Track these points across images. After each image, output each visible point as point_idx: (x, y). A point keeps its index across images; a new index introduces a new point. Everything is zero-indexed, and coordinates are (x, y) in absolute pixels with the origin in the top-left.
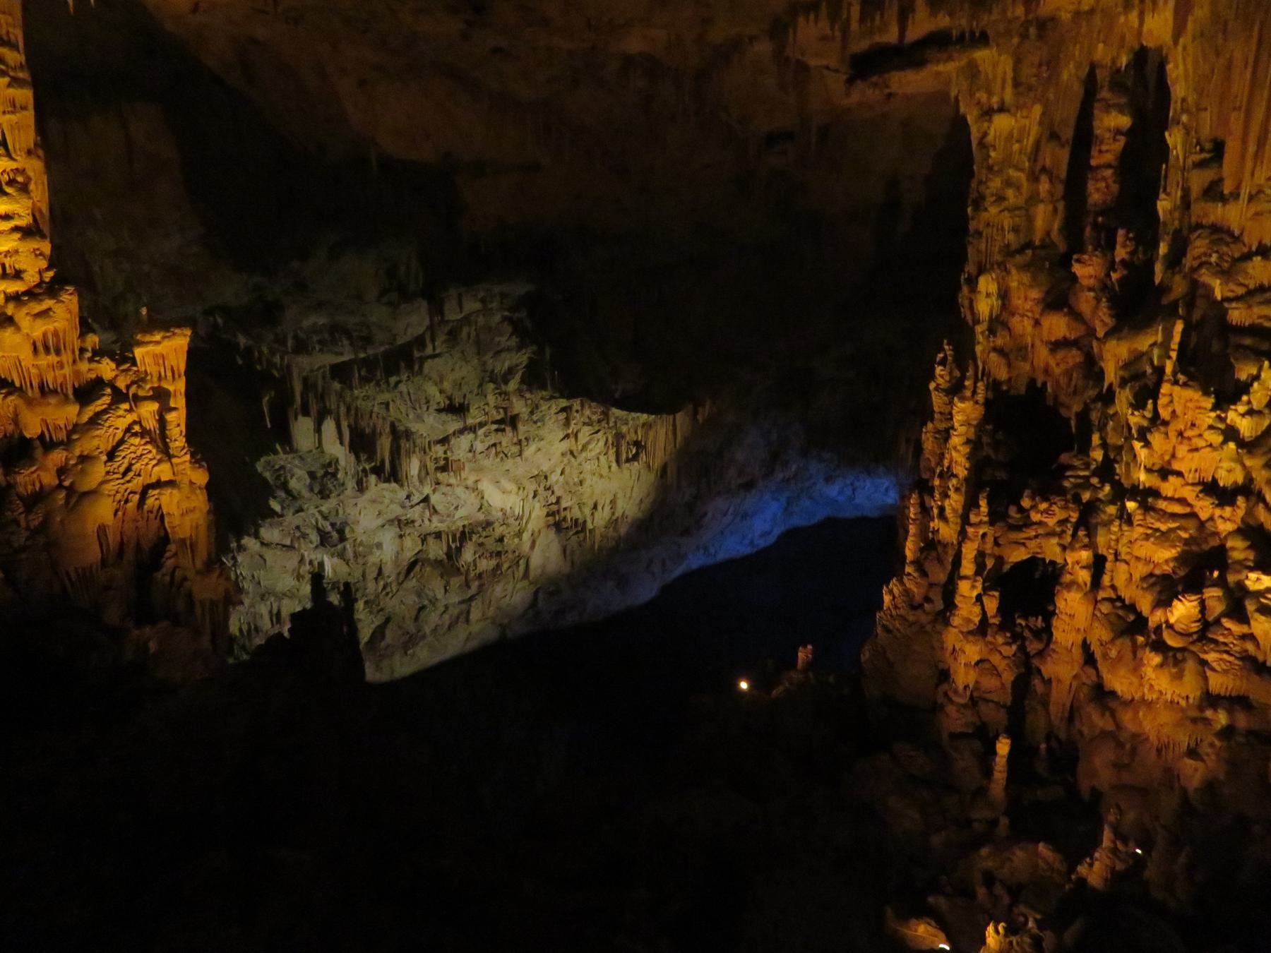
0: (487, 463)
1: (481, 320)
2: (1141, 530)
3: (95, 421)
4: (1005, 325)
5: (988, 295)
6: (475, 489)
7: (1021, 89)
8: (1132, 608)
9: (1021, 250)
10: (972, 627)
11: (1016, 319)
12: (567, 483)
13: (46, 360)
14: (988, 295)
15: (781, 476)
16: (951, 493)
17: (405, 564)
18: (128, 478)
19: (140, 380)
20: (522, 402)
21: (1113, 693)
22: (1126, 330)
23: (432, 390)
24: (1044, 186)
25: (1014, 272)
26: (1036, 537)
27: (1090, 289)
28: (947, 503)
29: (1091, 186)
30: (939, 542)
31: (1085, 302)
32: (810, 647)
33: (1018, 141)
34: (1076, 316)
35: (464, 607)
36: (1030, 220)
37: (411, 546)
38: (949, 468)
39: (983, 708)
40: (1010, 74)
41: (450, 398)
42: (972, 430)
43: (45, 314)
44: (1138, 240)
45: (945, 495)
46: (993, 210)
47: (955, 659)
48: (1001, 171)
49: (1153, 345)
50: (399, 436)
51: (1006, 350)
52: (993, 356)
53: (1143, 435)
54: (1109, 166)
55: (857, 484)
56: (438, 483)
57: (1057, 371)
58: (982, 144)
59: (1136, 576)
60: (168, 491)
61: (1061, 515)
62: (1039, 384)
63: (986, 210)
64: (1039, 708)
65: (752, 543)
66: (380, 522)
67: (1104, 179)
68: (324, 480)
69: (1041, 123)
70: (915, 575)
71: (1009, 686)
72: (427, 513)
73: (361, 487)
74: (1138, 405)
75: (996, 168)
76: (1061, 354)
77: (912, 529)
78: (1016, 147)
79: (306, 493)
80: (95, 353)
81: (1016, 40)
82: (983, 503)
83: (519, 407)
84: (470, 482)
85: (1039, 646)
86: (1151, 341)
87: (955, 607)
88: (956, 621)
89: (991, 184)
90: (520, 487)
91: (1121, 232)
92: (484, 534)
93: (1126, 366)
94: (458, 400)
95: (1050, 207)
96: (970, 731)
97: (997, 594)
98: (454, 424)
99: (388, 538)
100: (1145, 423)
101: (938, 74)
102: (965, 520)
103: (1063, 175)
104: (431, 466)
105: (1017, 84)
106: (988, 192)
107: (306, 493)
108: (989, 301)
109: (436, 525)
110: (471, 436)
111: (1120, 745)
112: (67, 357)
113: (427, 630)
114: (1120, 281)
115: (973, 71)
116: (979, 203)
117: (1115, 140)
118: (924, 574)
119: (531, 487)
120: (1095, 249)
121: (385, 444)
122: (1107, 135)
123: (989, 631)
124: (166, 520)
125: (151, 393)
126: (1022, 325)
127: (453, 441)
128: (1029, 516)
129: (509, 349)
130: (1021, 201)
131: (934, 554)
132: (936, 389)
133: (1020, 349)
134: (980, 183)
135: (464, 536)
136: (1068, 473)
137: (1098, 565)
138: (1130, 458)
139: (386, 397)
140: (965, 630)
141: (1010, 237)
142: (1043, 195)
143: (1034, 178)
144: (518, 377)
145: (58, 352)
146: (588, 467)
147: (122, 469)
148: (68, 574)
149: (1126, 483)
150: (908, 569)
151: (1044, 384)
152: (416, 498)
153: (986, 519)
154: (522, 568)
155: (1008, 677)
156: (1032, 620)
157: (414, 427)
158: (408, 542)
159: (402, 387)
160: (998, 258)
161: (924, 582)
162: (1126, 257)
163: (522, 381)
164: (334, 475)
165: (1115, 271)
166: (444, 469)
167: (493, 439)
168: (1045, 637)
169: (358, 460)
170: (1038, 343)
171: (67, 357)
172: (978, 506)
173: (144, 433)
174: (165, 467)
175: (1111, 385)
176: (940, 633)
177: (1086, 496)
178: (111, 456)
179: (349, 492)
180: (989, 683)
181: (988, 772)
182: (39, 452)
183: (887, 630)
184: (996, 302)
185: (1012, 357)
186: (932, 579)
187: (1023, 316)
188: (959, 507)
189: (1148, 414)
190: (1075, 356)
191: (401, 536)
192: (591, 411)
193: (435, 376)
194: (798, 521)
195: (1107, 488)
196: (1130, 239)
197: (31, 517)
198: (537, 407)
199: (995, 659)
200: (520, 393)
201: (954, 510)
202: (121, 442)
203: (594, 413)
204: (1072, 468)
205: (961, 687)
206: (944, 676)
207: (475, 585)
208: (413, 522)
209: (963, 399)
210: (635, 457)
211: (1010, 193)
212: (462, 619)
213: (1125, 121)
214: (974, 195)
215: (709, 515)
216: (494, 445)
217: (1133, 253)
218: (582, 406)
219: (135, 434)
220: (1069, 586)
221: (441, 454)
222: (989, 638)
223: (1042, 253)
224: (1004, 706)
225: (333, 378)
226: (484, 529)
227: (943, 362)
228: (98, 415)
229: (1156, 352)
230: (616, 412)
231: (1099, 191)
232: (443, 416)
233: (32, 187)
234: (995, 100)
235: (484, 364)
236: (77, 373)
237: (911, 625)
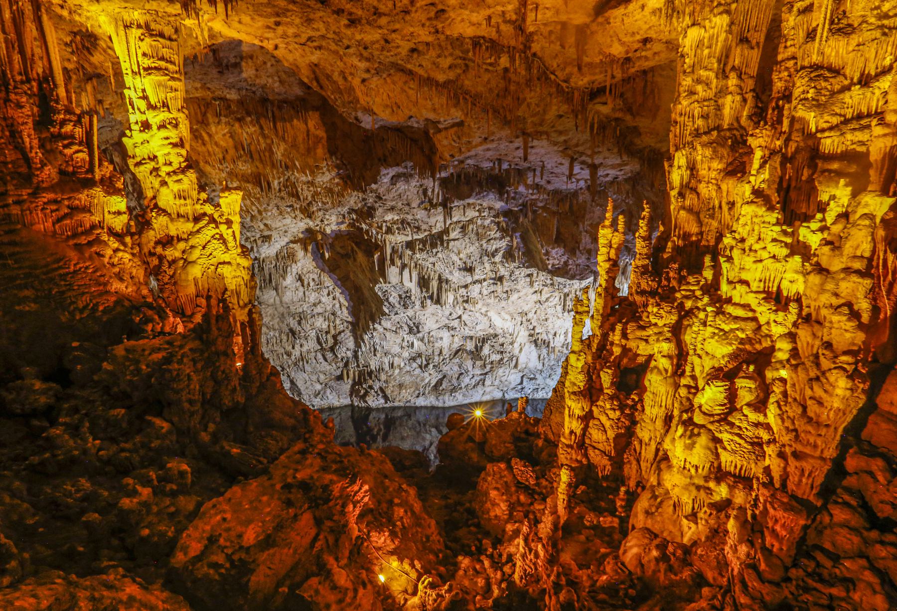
0: (489, 301)
6: (486, 315)
80: (204, 201)
84: (483, 311)
104: (460, 300)
113: (463, 385)
127: (470, 287)
135: (484, 340)
145: (185, 199)
152: (454, 316)
158: (456, 339)
166: (467, 301)
221: (465, 294)
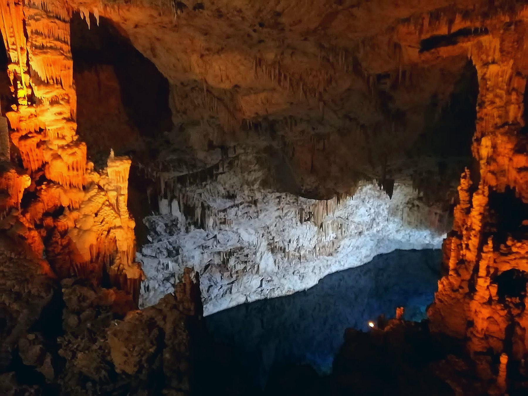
0: (242, 221)
1: (243, 158)
3: (90, 200)
4: (495, 160)
5: (487, 147)
6: (237, 233)
7: (505, 53)
9: (503, 126)
10: (485, 301)
12: (278, 231)
13: (72, 173)
14: (487, 147)
16: (472, 237)
17: (204, 266)
18: (102, 224)
19: (109, 183)
20: (260, 194)
23: (221, 188)
24: (514, 97)
25: (499, 136)
26: (515, 259)
28: (470, 242)
30: (466, 260)
32: (402, 308)
33: (502, 76)
35: (229, 286)
36: (507, 112)
37: (206, 259)
38: (470, 226)
39: (491, 340)
40: (498, 47)
41: (228, 192)
42: (482, 208)
43: (73, 154)
45: (469, 238)
46: (489, 108)
47: (477, 316)
48: (493, 90)
50: (205, 208)
51: (495, 172)
52: (489, 175)
56: (221, 230)
57: (521, 181)
58: (483, 78)
60: (119, 230)
62: (511, 188)
63: (485, 108)
64: (520, 342)
66: (195, 246)
68: (172, 228)
69: (512, 68)
70: (455, 275)
71: (503, 330)
72: (215, 243)
73: (187, 231)
76: (523, 174)
77: (453, 254)
78: (500, 79)
79: (163, 233)
81: (502, 31)
82: (490, 243)
83: (258, 196)
84: (235, 229)
85: (519, 312)
87: (476, 291)
88: (477, 297)
89: (487, 96)
90: (257, 232)
92: (240, 253)
94: (231, 193)
95: (517, 106)
96: (485, 351)
97: (496, 285)
98: (229, 203)
99: (197, 253)
101: (462, 47)
102: (480, 250)
103: (523, 92)
104: (218, 222)
105: (502, 51)
106: (486, 100)
107: (163, 233)
109: (219, 248)
110: (237, 208)
112: (80, 172)
113: (213, 296)
115: (480, 46)
118: (459, 275)
119: (261, 232)
121: (198, 211)
123: (493, 303)
124: (118, 242)
125: (114, 188)
126: (503, 161)
127: (228, 210)
128: (511, 249)
129: (255, 171)
130: (502, 104)
131: (463, 266)
132: (461, 189)
133: (502, 171)
134: (482, 96)
135: (230, 254)
139: (200, 191)
140: (482, 302)
141: (498, 120)
142: (513, 101)
143: (509, 93)
144: (258, 183)
145: (77, 170)
146: (287, 223)
147: (101, 221)
148: (77, 265)
150: (451, 273)
151: (514, 188)
152: (211, 236)
153: (492, 250)
154: (256, 269)
155: (503, 326)
156: (514, 299)
157: (212, 204)
158: (205, 256)
159: (208, 187)
160: (491, 129)
161: (459, 279)
163: (260, 184)
164: (176, 225)
166: (224, 223)
167: (246, 210)
168: (521, 307)
169: (187, 219)
170: (511, 168)
171: (80, 172)
172: (488, 244)
173: (110, 205)
174: (118, 220)
176: (469, 304)
178: (96, 215)
179: (182, 233)
180: (494, 328)
181: (496, 372)
182: (67, 212)
183: (441, 301)
184: (490, 150)
185: (498, 175)
187: (504, 156)
191: (202, 253)
192: (290, 198)
193: (222, 182)
197: (63, 240)
198: (266, 196)
199: (496, 317)
200: (259, 190)
201: (474, 246)
202: (101, 208)
203: (291, 199)
205: (480, 329)
206: (471, 324)
207: (234, 276)
208: (209, 247)
209: (478, 194)
210: (309, 219)
211: (497, 100)
212: (228, 292)
214: (479, 101)
215: (341, 247)
216: (246, 213)
218: (286, 196)
219: (107, 205)
222: (493, 307)
223: (513, 127)
224: (501, 340)
225: (178, 182)
226: (239, 251)
227: (465, 177)
228: (92, 197)
230: (301, 199)
232: (225, 200)
233: (71, 101)
234: (490, 59)
235: (244, 176)
236: (84, 179)
237: (453, 299)
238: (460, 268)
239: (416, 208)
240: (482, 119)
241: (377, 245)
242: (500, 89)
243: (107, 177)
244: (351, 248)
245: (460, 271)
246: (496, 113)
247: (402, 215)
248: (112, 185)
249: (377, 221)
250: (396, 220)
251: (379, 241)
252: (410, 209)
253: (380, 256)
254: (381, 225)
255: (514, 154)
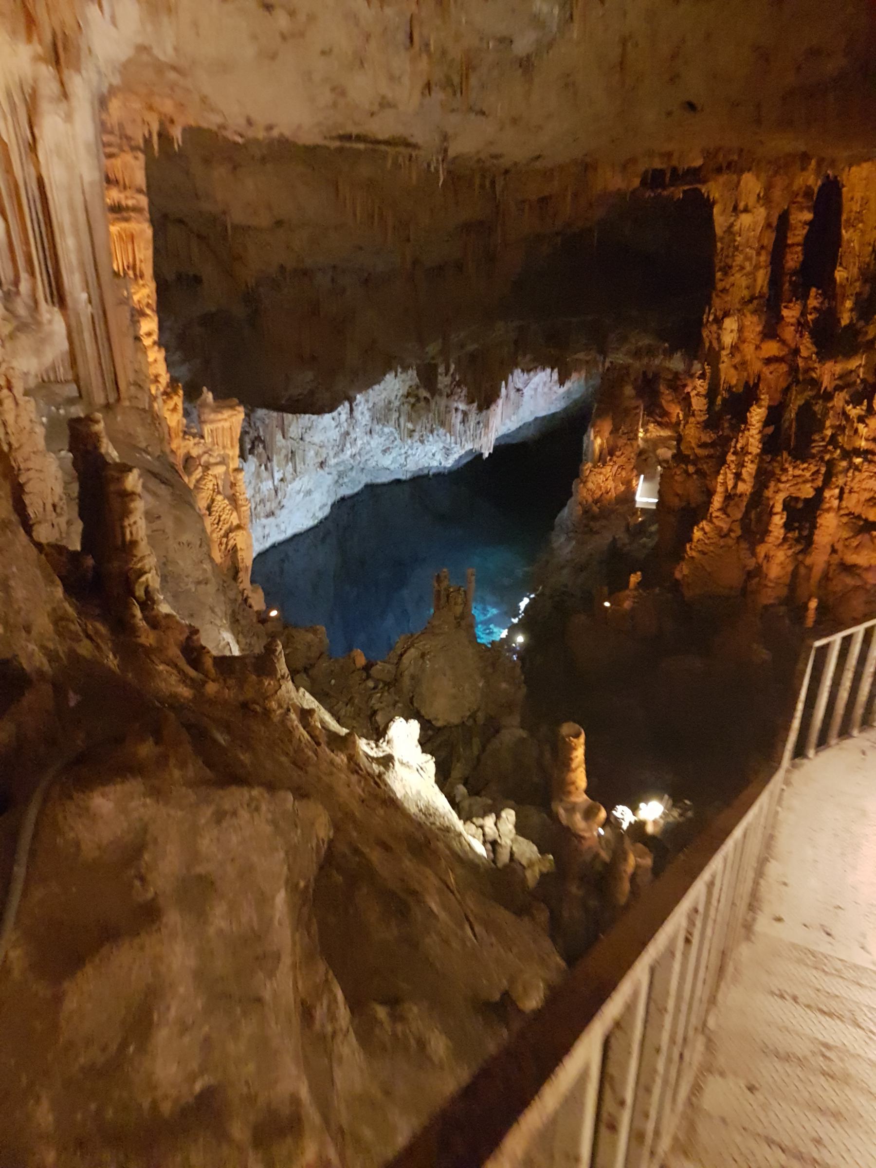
2: (867, 474)
8: (859, 517)
9: (750, 301)
11: (746, 344)
14: (732, 331)
15: (349, 453)
21: (855, 566)
22: (840, 357)
25: (748, 315)
27: (792, 325)
28: (744, 471)
29: (789, 257)
31: (789, 333)
33: (754, 231)
34: (783, 342)
38: (742, 448)
44: (825, 295)
45: (741, 465)
46: (738, 276)
49: (860, 366)
52: (733, 371)
53: (861, 419)
54: (798, 245)
55: (410, 452)
58: (729, 229)
59: (863, 499)
60: (240, 533)
61: (813, 469)
65: (314, 515)
67: (797, 253)
70: (723, 516)
74: (855, 401)
75: (740, 248)
76: (772, 367)
86: (858, 364)
91: (813, 291)
93: (840, 377)
100: (863, 413)
106: (734, 264)
108: (732, 335)
111: (868, 591)
114: (816, 321)
116: (727, 270)
117: (804, 228)
118: (728, 516)
120: (797, 299)
122: (800, 224)
124: (239, 553)
125: (219, 459)
126: (749, 350)
131: (732, 503)
136: (813, 445)
137: (840, 497)
138: (852, 433)
143: (758, 254)
149: (847, 447)
160: (738, 306)
161: (729, 520)
162: (818, 305)
165: (811, 314)
173: (219, 493)
175: (826, 388)
177: (827, 457)
184: (735, 335)
186: (735, 518)
187: (749, 342)
188: (754, 472)
189: (864, 408)
190: (784, 368)
194: (347, 491)
195: (838, 451)
196: (820, 295)
201: (750, 474)
202: (213, 501)
204: (814, 441)
211: (747, 264)
213: (808, 216)
214: (718, 264)
217: (822, 303)
220: (828, 510)
228: (198, 481)
229: (861, 370)
231: (793, 259)
237: (722, 547)
238: (727, 506)
239: (423, 404)
240: (724, 290)
241: (337, 482)
242: (751, 247)
243: (202, 441)
244: (302, 494)
245: (729, 510)
246: (744, 282)
247: (398, 419)
248: (215, 454)
249: (353, 436)
250: (386, 430)
251: (340, 475)
252: (413, 405)
253: (343, 499)
254: (359, 442)
255: (762, 341)
